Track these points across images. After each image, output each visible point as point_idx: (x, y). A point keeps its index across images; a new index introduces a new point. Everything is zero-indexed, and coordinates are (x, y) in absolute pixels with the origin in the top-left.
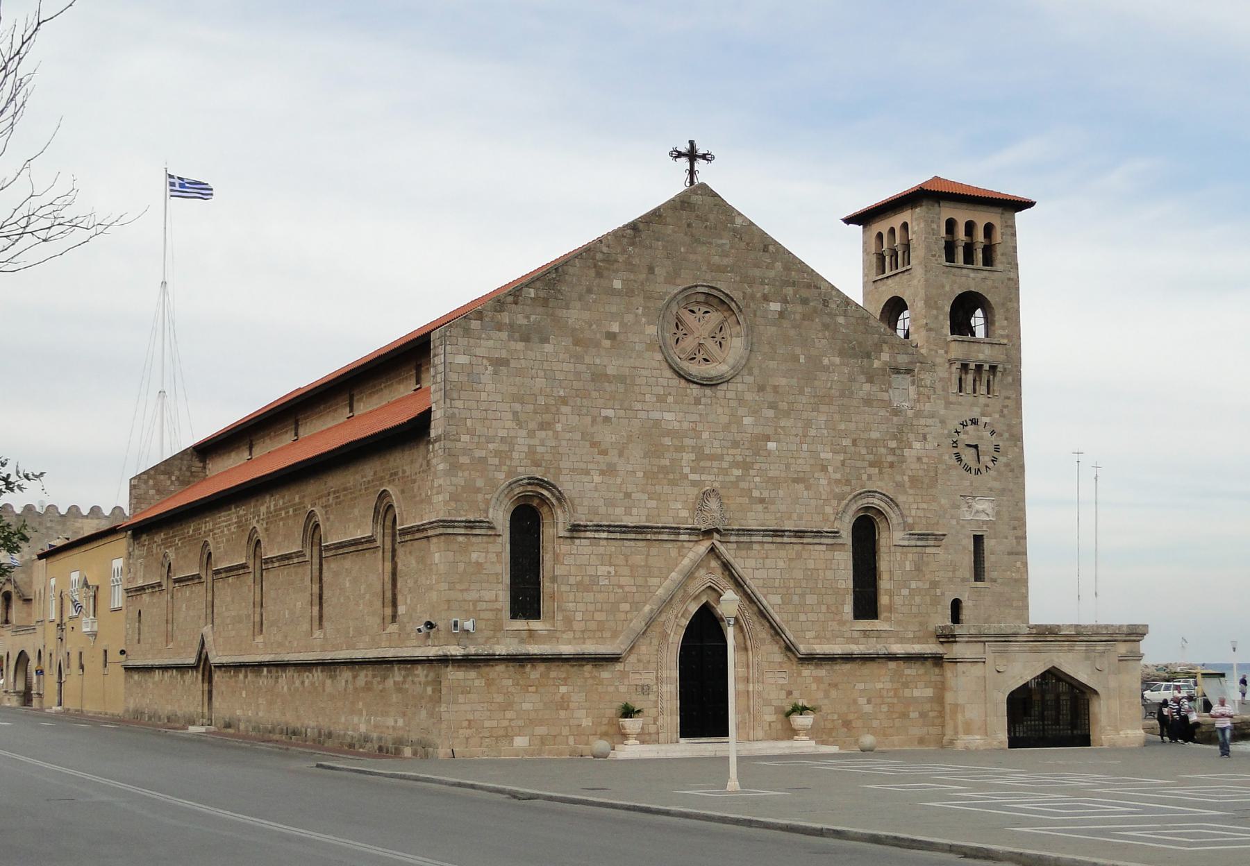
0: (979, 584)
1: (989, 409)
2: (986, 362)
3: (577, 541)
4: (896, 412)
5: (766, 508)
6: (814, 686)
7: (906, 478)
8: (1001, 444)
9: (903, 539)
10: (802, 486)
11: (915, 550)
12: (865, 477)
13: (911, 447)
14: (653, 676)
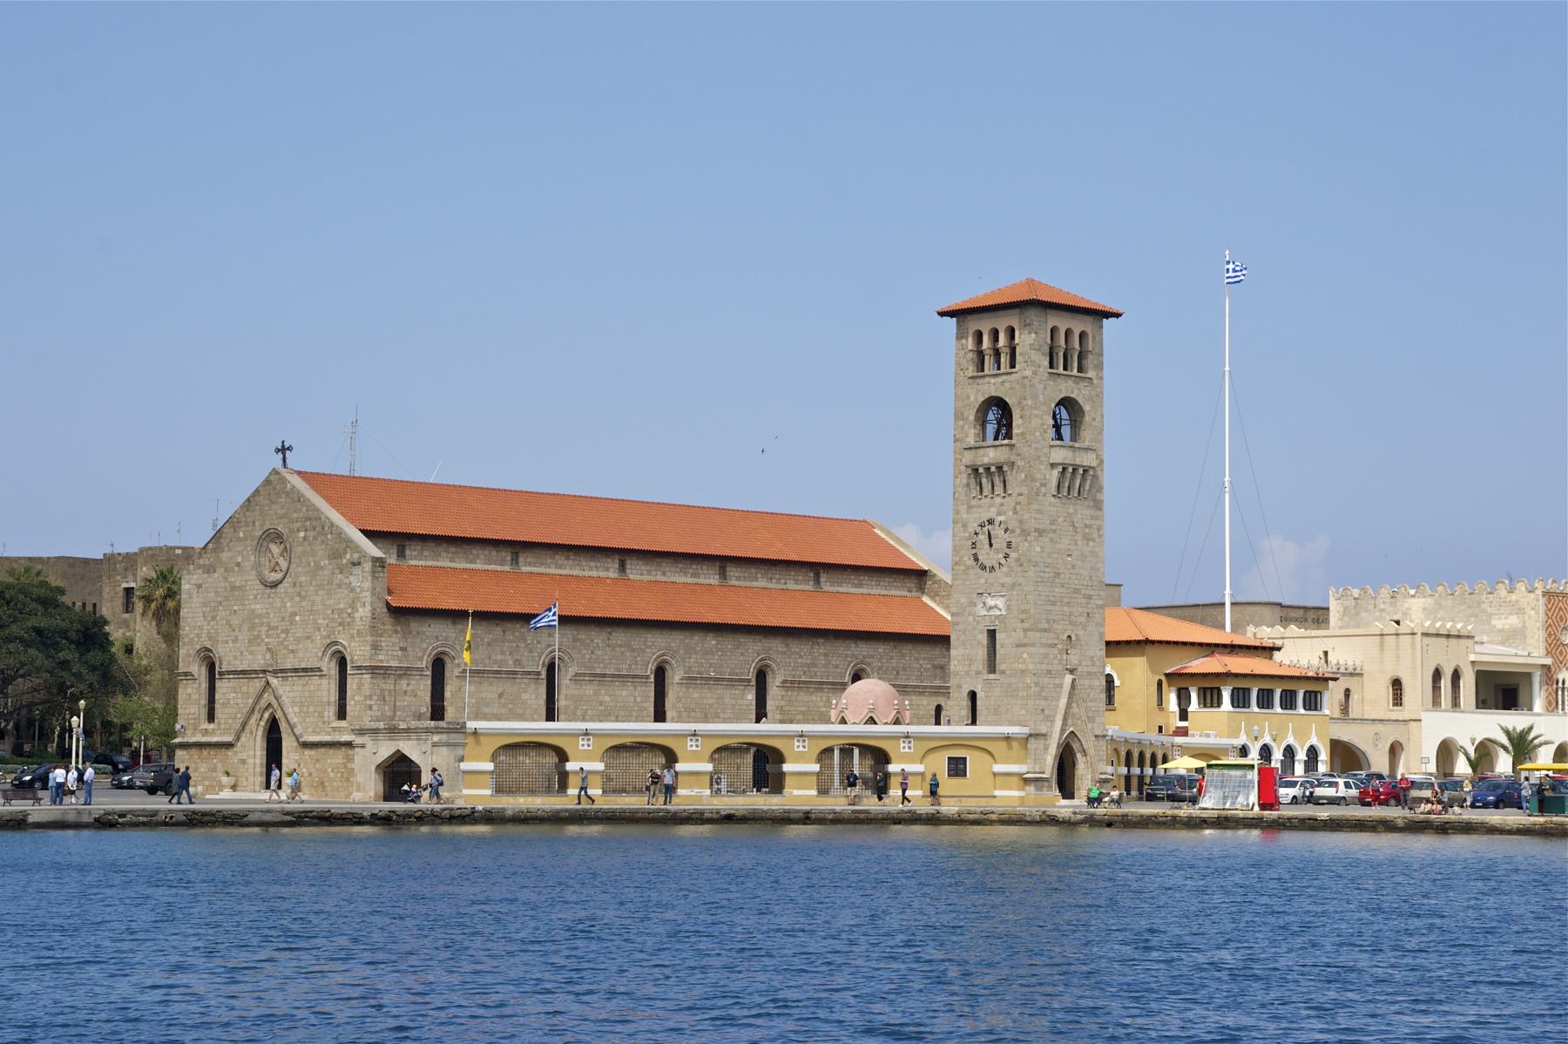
0: (992, 676)
1: (1005, 508)
4: (352, 590)
8: (1013, 540)
10: (309, 641)
11: (358, 676)
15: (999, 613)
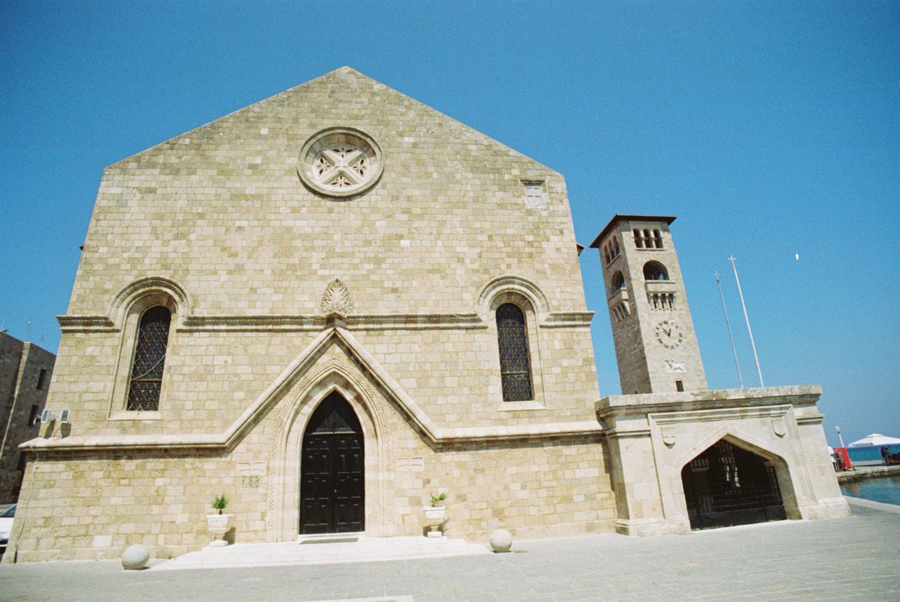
1: (672, 316)
2: (666, 292)
3: (196, 334)
5: (399, 297)
6: (456, 473)
7: (547, 266)
8: (682, 332)
9: (548, 320)
10: (438, 276)
12: (503, 266)
13: (548, 240)
14: (263, 467)
15: (681, 372)
